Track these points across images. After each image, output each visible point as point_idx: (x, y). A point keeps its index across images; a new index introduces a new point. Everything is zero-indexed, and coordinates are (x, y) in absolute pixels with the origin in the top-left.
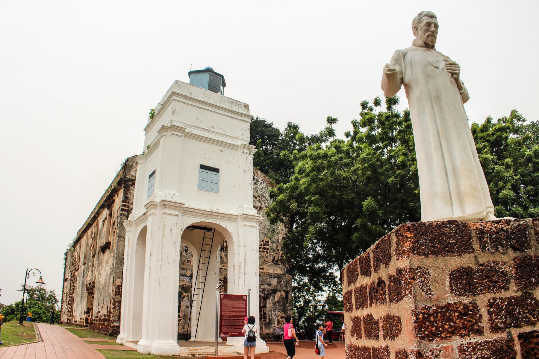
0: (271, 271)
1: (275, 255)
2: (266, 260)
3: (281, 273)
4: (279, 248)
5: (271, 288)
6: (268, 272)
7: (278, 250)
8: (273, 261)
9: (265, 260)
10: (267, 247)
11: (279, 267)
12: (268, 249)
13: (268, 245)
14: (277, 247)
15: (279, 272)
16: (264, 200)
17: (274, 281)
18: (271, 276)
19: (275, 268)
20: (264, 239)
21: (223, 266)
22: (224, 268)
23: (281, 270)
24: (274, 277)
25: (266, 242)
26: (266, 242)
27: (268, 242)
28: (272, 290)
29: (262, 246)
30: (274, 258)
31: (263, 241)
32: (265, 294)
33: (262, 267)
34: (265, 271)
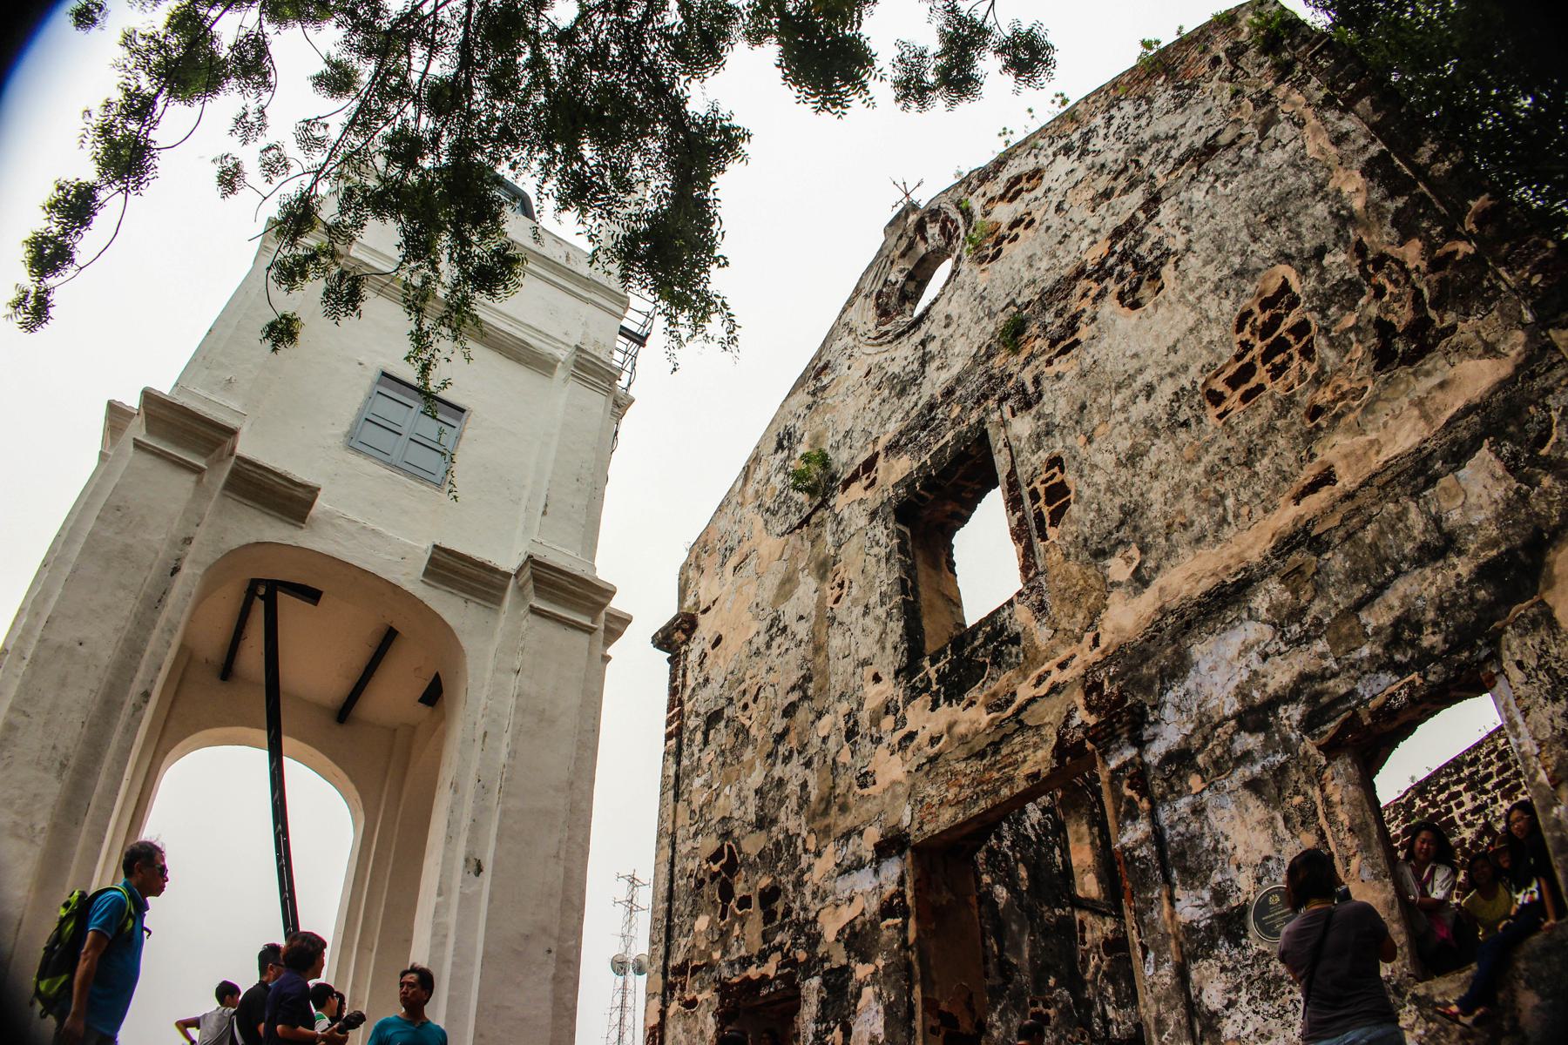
0: (1402, 434)
1: (1373, 311)
2: (1324, 396)
3: (1504, 369)
4: (1381, 239)
5: (1463, 567)
7: (1381, 261)
8: (1384, 358)
9: (1315, 412)
10: (1291, 319)
11: (1463, 349)
12: (1301, 329)
13: (1294, 302)
14: (1360, 249)
15: (1476, 377)
17: (1478, 491)
18: (1417, 473)
21: (1040, 680)
22: (1044, 689)
23: (1490, 350)
24: (1458, 455)
27: (1285, 287)
28: (1485, 573)
29: (1259, 346)
30: (1384, 328)
32: (1424, 659)
33: (1308, 474)
34: (1347, 480)
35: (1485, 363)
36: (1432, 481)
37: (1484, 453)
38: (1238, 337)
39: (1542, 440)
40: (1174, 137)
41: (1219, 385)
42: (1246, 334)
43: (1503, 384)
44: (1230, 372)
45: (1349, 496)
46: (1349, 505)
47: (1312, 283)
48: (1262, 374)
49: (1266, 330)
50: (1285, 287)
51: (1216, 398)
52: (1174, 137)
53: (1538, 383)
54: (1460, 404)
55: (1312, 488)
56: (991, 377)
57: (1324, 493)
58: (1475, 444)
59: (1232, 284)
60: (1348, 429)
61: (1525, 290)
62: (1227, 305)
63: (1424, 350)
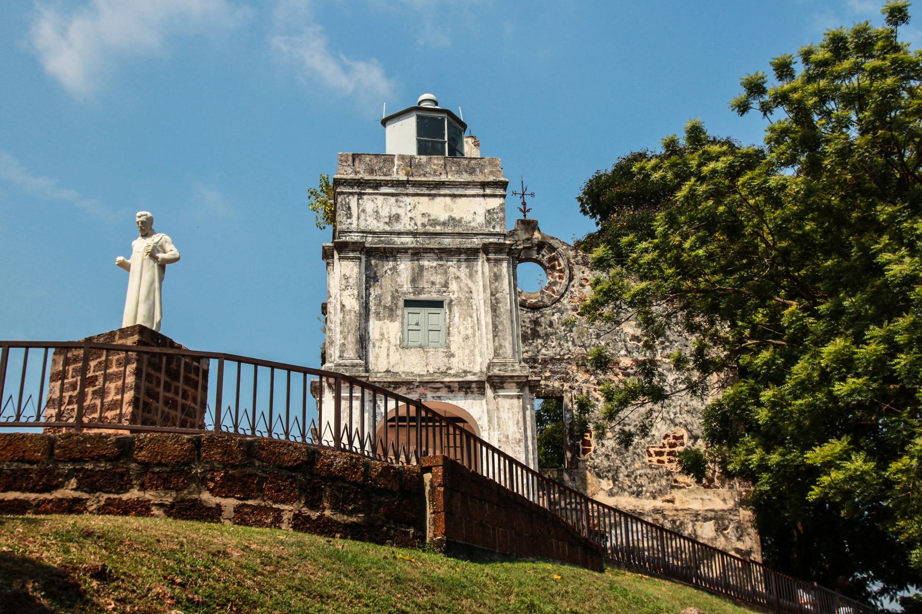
0: (696, 506)
3: (725, 508)
6: (686, 506)
13: (682, 444)
15: (718, 505)
16: (662, 343)
19: (705, 497)
20: (669, 432)
23: (724, 500)
24: (706, 519)
25: (675, 438)
26: (675, 438)
27: (682, 437)
29: (667, 449)
31: (666, 436)
33: (668, 497)
35: (722, 503)
36: (697, 520)
37: (712, 522)
38: (663, 441)
39: (725, 529)
40: (671, 342)
41: (652, 450)
42: (665, 442)
43: (723, 510)
44: (658, 450)
45: (677, 510)
46: (675, 513)
47: (690, 444)
48: (665, 458)
49: (672, 445)
50: (682, 437)
51: (650, 455)
52: (671, 342)
53: (731, 516)
54: (711, 507)
55: (668, 501)
56: (568, 374)
57: (671, 504)
58: (711, 519)
59: (668, 422)
60: (683, 493)
61: (740, 494)
62: (664, 427)
63: (708, 487)
